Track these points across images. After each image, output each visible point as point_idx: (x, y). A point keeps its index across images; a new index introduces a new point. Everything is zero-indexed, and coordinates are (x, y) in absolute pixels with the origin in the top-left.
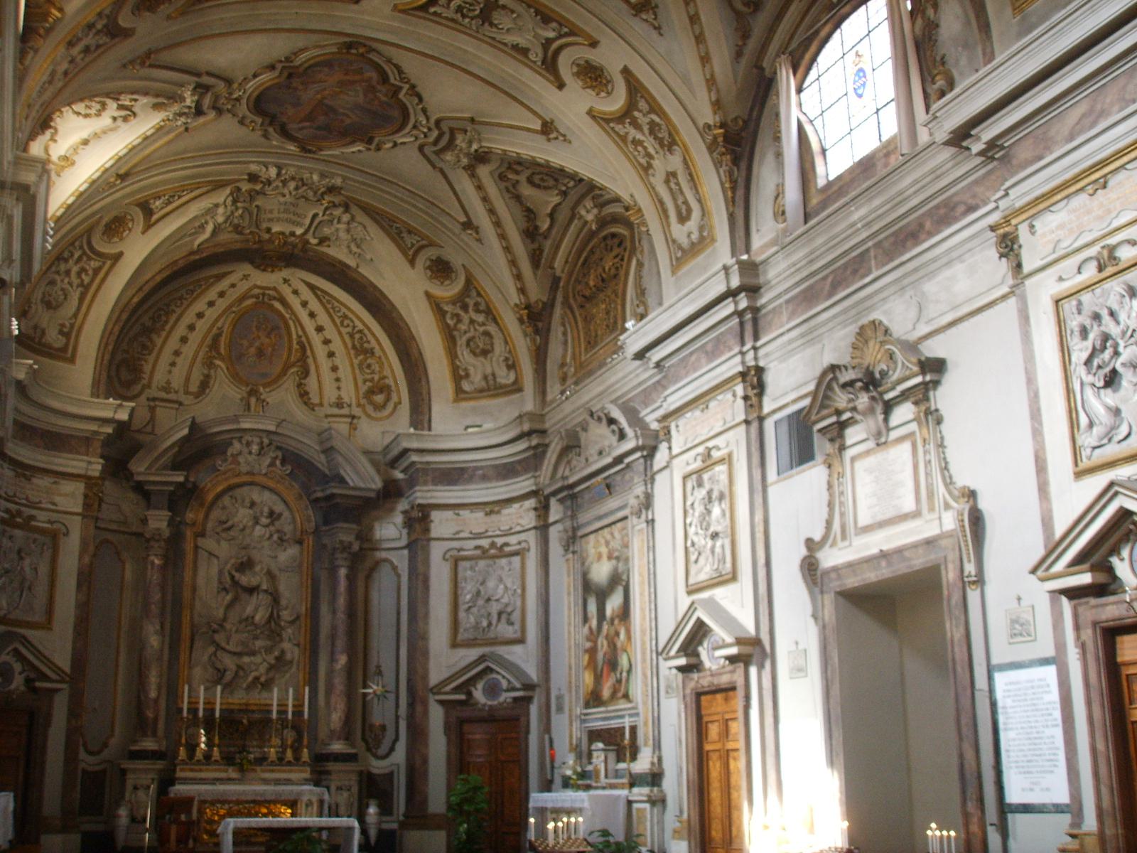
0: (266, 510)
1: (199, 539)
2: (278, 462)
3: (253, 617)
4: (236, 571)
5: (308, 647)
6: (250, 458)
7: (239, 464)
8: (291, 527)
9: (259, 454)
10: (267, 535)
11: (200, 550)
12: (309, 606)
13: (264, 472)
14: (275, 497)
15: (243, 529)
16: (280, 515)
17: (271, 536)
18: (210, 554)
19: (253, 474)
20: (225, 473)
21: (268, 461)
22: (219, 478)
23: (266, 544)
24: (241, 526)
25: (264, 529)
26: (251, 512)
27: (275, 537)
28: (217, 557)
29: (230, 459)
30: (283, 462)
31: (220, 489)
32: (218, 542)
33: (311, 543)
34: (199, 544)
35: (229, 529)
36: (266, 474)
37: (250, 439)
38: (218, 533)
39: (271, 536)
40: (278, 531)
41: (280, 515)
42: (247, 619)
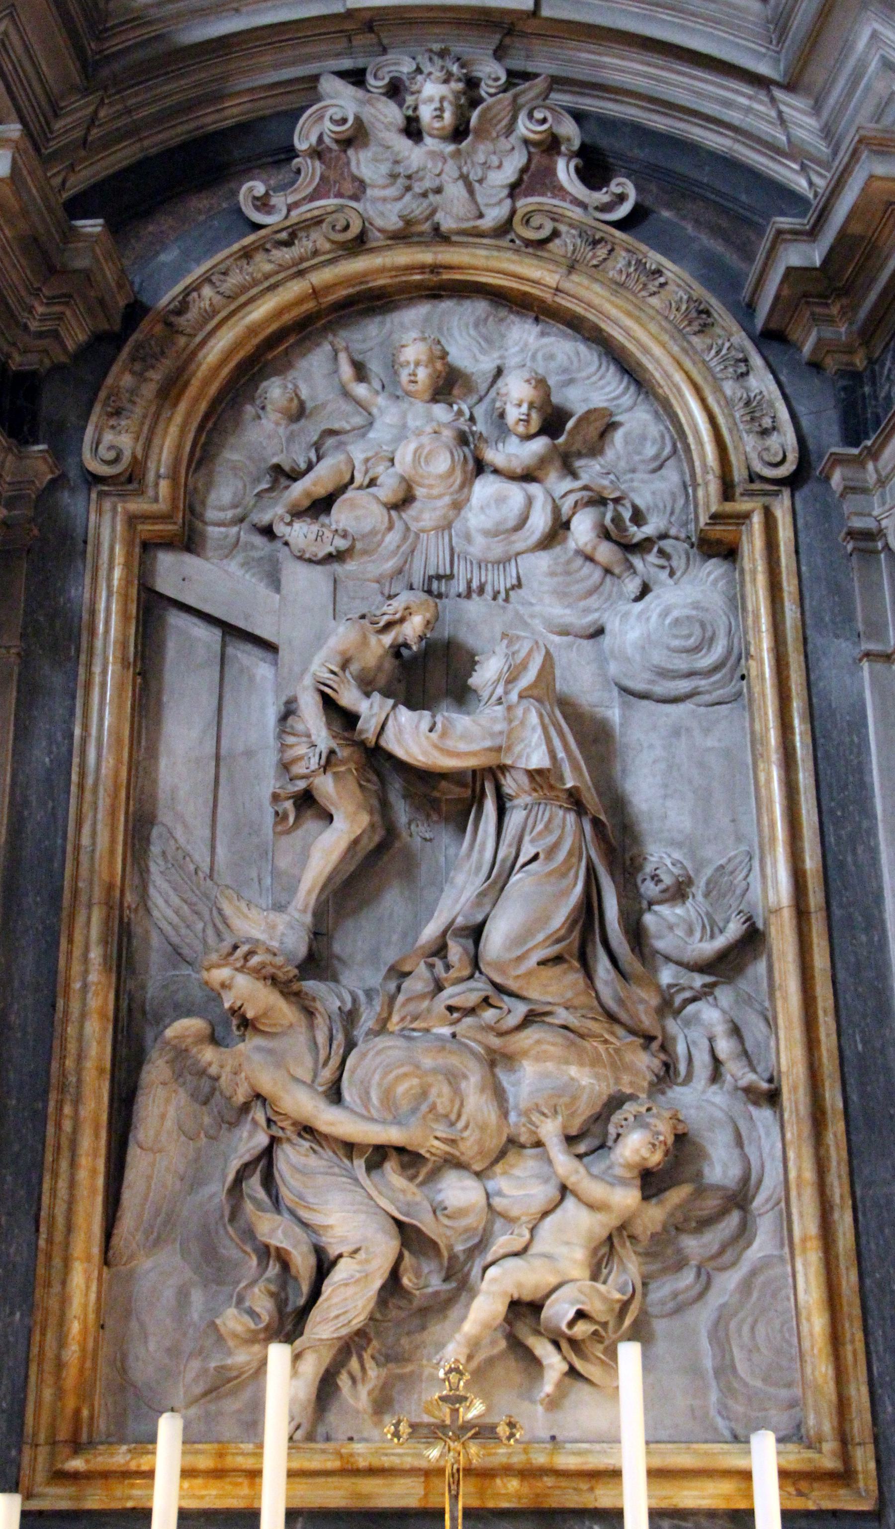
1: (166, 560)
3: (476, 932)
4: (367, 686)
5: (833, 1098)
7: (360, 187)
8: (671, 477)
9: (459, 133)
10: (540, 521)
11: (176, 620)
12: (811, 863)
13: (494, 215)
19: (440, 237)
22: (263, 264)
24: (388, 489)
25: (516, 493)
26: (440, 411)
28: (269, 647)
32: (275, 581)
34: (166, 585)
36: (504, 229)
37: (406, 67)
38: (268, 532)
40: (598, 501)
42: (440, 950)
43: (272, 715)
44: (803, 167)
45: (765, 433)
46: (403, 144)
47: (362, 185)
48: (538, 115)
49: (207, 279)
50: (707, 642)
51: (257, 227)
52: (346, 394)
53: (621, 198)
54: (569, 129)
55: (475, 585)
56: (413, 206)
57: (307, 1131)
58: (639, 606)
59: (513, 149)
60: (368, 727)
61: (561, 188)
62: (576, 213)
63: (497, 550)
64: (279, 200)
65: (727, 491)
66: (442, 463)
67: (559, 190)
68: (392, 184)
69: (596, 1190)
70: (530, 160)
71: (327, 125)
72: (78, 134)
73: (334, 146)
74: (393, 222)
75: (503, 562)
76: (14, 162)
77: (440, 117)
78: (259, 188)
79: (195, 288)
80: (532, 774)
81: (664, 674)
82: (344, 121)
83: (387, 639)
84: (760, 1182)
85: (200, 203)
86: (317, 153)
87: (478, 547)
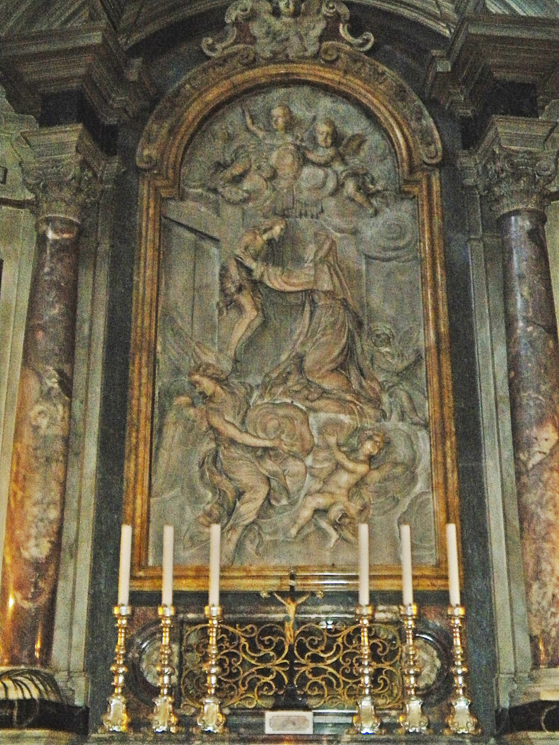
0: (323, 128)
2: (343, 31)
5: (451, 426)
6: (277, 24)
7: (254, 40)
9: (296, 14)
10: (331, 184)
13: (312, 49)
14: (343, 108)
15: (274, 176)
16: (360, 140)
17: (340, 186)
18: (203, 236)
20: (225, 60)
21: (320, 27)
23: (330, 204)
25: (320, 173)
27: (350, 187)
29: (233, 33)
30: (355, 31)
31: (211, 96)
33: (436, 187)
35: (237, 180)
36: (316, 56)
39: (340, 186)
41: (360, 140)
43: (217, 270)
44: (447, 24)
45: (429, 144)
46: (272, 20)
47: (255, 38)
48: (331, 5)
49: (188, 81)
50: (402, 236)
51: (209, 58)
52: (247, 129)
53: (368, 41)
54: (344, 10)
55: (303, 212)
56: (277, 47)
57: (233, 442)
58: (373, 220)
59: (320, 20)
60: (257, 275)
61: (341, 37)
62: (348, 48)
63: (314, 196)
64: (218, 46)
65: (412, 170)
66: (289, 160)
67: (340, 38)
68: (268, 37)
69: (350, 465)
70: (327, 26)
71: (239, 11)
72: (131, 20)
73: (242, 22)
74: (268, 55)
75: (316, 203)
76: (103, 36)
77: (288, 7)
78: (210, 41)
79: (183, 86)
80: (326, 293)
81: (385, 249)
82: (246, 10)
83: (265, 237)
84: (420, 460)
85: (184, 49)
86: (236, 23)
87: (305, 195)
